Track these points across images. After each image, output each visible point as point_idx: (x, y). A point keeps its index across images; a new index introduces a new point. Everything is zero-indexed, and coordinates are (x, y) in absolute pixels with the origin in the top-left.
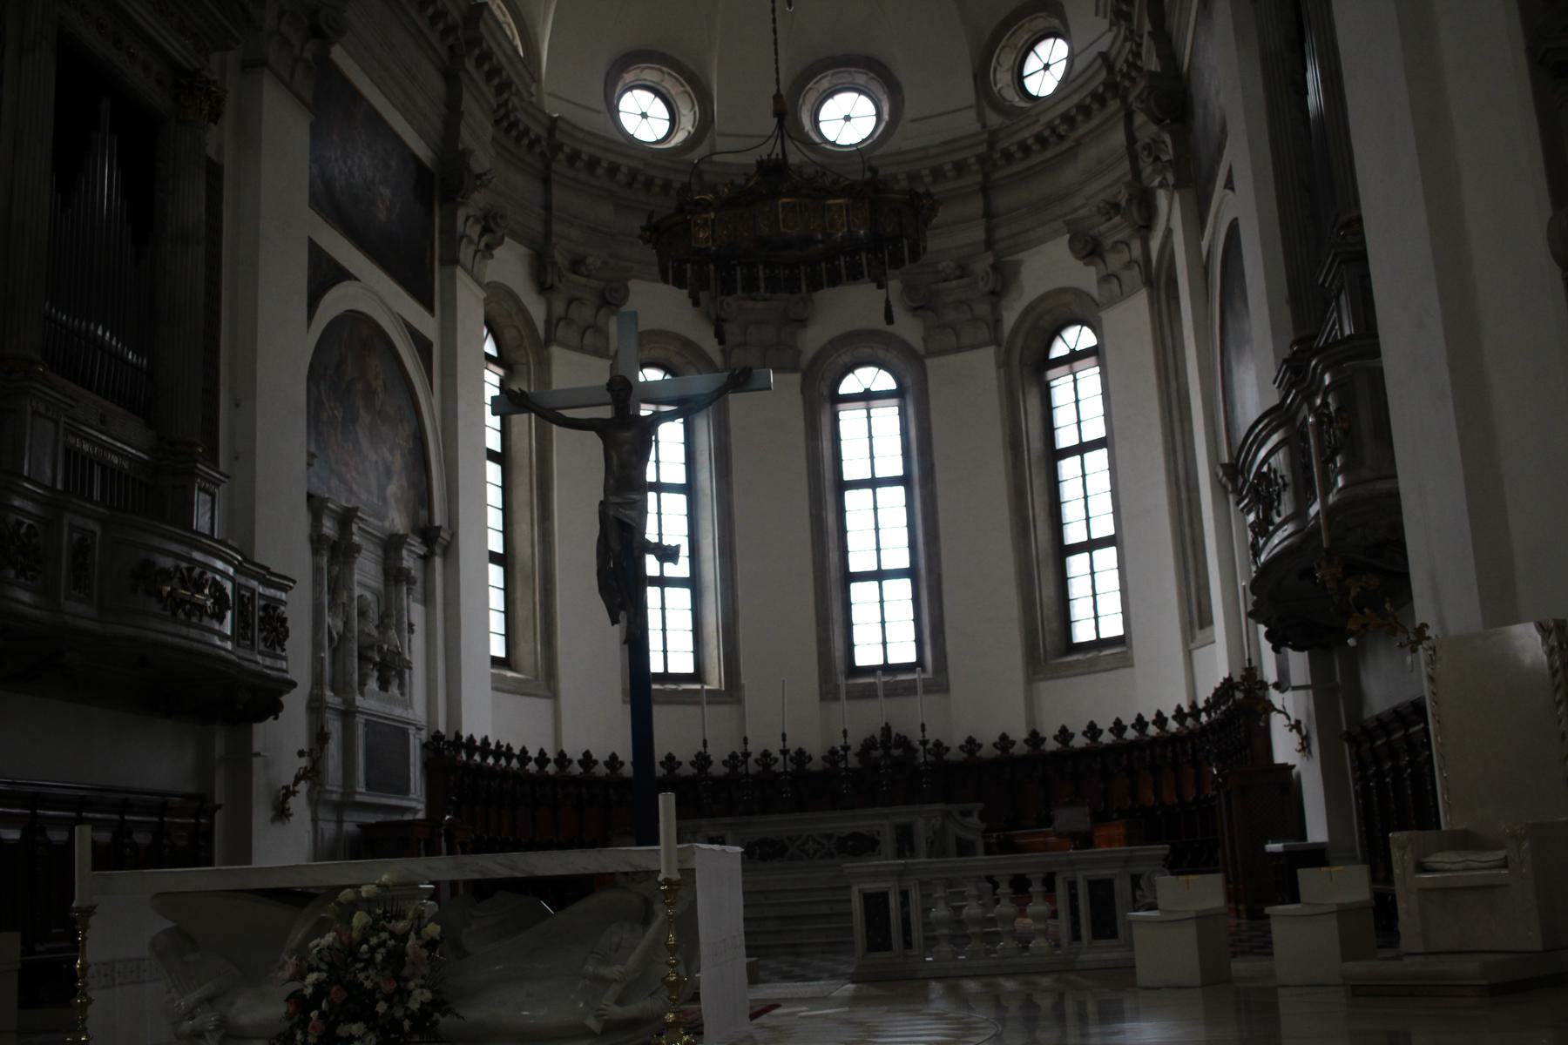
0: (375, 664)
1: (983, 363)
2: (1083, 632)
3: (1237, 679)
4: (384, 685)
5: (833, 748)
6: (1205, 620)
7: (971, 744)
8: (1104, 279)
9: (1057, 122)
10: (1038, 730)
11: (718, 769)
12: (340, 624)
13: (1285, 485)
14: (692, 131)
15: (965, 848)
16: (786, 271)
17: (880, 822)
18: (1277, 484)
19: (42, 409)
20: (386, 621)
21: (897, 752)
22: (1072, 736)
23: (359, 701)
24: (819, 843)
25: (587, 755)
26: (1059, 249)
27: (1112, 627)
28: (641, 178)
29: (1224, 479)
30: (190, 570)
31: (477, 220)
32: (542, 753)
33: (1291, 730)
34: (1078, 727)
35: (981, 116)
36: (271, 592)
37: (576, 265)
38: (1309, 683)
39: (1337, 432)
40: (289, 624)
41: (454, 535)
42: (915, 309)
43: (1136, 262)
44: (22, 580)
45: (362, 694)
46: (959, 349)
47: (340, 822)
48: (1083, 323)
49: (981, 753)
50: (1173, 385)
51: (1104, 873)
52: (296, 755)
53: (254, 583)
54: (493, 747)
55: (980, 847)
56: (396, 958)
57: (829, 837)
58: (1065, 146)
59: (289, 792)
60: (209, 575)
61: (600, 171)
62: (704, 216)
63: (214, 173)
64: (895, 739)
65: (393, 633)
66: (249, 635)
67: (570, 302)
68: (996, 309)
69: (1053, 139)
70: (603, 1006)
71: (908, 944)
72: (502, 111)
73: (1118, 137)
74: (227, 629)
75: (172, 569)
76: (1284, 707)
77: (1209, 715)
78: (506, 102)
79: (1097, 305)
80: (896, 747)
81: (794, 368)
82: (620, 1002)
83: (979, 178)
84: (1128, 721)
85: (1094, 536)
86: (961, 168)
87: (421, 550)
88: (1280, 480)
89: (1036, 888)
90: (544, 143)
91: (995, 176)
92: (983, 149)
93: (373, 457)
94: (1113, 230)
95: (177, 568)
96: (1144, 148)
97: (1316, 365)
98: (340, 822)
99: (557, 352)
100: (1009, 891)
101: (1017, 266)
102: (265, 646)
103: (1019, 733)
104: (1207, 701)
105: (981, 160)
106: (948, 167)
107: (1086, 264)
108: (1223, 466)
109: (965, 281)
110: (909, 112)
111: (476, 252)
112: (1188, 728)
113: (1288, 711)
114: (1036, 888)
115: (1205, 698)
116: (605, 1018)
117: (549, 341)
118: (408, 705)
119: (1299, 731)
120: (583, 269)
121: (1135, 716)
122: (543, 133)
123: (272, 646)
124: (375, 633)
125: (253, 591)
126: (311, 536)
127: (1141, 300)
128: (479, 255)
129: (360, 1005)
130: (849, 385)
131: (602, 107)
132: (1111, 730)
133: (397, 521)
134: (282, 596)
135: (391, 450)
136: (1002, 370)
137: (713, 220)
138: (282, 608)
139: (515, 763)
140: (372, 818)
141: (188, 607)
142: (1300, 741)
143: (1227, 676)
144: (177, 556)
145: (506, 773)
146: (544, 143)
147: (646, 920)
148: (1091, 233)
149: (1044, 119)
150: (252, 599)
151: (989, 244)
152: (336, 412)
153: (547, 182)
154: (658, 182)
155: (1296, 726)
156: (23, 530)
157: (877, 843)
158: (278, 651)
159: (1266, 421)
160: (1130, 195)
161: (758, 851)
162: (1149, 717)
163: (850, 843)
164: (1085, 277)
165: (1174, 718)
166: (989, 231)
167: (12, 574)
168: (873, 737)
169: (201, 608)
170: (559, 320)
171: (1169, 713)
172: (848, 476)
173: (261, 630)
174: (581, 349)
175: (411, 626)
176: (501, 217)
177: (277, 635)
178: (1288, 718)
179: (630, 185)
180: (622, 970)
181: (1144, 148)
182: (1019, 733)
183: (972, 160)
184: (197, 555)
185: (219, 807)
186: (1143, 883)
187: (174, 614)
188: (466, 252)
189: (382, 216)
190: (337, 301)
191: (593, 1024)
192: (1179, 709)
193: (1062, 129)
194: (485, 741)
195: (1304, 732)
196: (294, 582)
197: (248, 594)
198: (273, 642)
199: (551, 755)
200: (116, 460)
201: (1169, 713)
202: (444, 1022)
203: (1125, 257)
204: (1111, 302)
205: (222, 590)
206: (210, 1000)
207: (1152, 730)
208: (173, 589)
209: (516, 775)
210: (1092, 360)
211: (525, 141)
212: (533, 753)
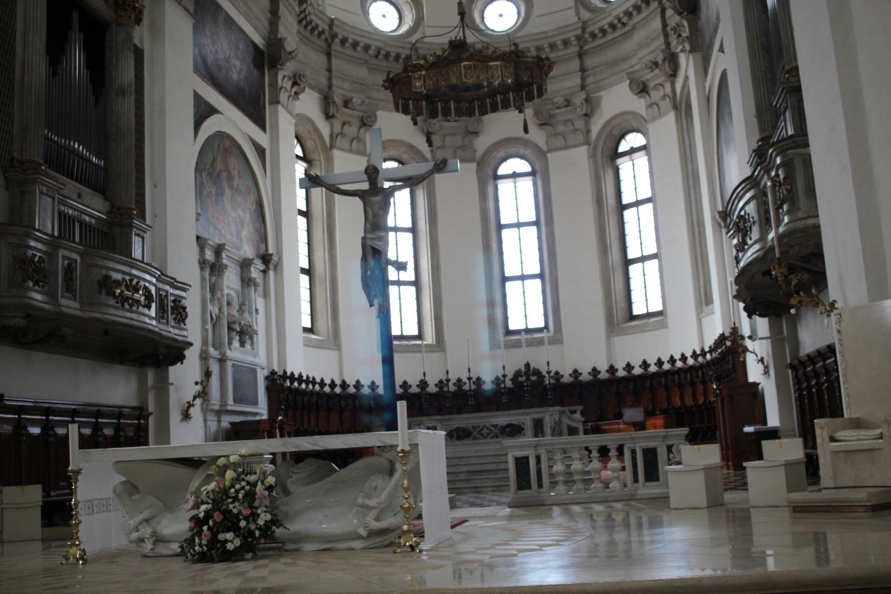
0: (237, 332)
1: (580, 155)
2: (638, 309)
3: (727, 334)
4: (242, 344)
5: (497, 376)
6: (709, 301)
8: (650, 106)
9: (622, 15)
10: (614, 365)
11: (432, 389)
12: (216, 310)
13: (754, 222)
14: (412, 24)
15: (572, 431)
16: (467, 104)
17: (525, 418)
18: (750, 222)
19: (45, 190)
20: (243, 307)
21: (533, 378)
22: (633, 368)
23: (229, 353)
24: (490, 430)
25: (358, 382)
26: (623, 88)
27: (656, 305)
28: (383, 53)
29: (719, 220)
30: (131, 280)
31: (290, 78)
32: (333, 381)
33: (758, 363)
34: (636, 363)
35: (578, 13)
36: (177, 292)
37: (347, 103)
38: (768, 335)
39: (784, 191)
40: (187, 310)
41: (280, 259)
42: (541, 125)
43: (668, 96)
44: (37, 287)
45: (230, 349)
46: (567, 147)
47: (219, 421)
48: (637, 131)
49: (581, 378)
50: (690, 166)
51: (651, 444)
52: (194, 385)
53: (167, 288)
54: (305, 378)
55: (581, 430)
56: (250, 496)
57: (496, 426)
58: (626, 29)
59: (190, 405)
60: (142, 283)
61: (359, 49)
62: (419, 73)
63: (139, 54)
64: (533, 371)
65: (246, 315)
66: (166, 317)
67: (344, 124)
68: (587, 123)
69: (619, 25)
70: (368, 522)
71: (540, 485)
72: (303, 15)
73: (657, 24)
74: (153, 312)
75: (121, 280)
76: (754, 350)
77: (711, 355)
78: (304, 10)
79: (646, 121)
80: (534, 374)
81: (472, 160)
82: (377, 519)
83: (577, 49)
84: (665, 359)
85: (645, 254)
86: (566, 43)
87: (262, 267)
88: (751, 220)
89: (613, 453)
90: (327, 33)
91: (586, 48)
92: (579, 32)
93: (233, 215)
94: (655, 78)
95: (124, 279)
96: (672, 30)
97: (772, 154)
98: (219, 421)
99: (336, 153)
100: (598, 455)
101: (599, 99)
102: (175, 323)
103: (603, 367)
104: (710, 347)
105: (578, 38)
106: (559, 43)
107: (639, 97)
108: (719, 212)
109: (569, 108)
110: (536, 11)
111: (289, 96)
112: (699, 362)
113: (756, 352)
114: (613, 453)
115: (709, 345)
116: (369, 528)
117: (332, 147)
118: (256, 355)
119: (763, 363)
120: (350, 105)
121: (669, 356)
122: (326, 28)
123: (179, 322)
124: (236, 314)
125: (167, 292)
126: (199, 260)
127: (671, 117)
128: (291, 98)
129: (231, 523)
130: (503, 169)
131: (359, 11)
132: (655, 364)
133: (248, 251)
134: (183, 294)
135: (243, 211)
136: (591, 160)
137: (424, 76)
138: (184, 301)
139: (317, 387)
140: (237, 419)
141: (130, 301)
142: (763, 369)
143: (721, 332)
144: (123, 273)
145: (312, 393)
146: (327, 33)
147: (391, 473)
148: (642, 79)
149: (614, 14)
150: (166, 296)
151: (583, 87)
152: (211, 189)
153: (329, 55)
154: (393, 55)
155: (762, 360)
156: (36, 259)
157: (523, 429)
158: (182, 325)
159: (743, 185)
160: (664, 57)
161: (455, 435)
162: (677, 356)
163: (507, 430)
164: (639, 105)
165: (692, 357)
166: (583, 79)
167: (31, 284)
168: (520, 369)
169: (138, 302)
170: (338, 135)
171: (688, 354)
172: (503, 222)
173: (172, 314)
174: (350, 151)
175: (257, 310)
176: (303, 76)
177: (181, 317)
178: (757, 356)
179: (376, 56)
180: (378, 501)
181: (672, 30)
182: (603, 367)
183: (573, 39)
184: (135, 272)
185: (151, 414)
186: (674, 450)
187: (123, 305)
188: (283, 97)
189: (235, 77)
190: (211, 126)
191: (363, 532)
192: (694, 352)
193: (625, 20)
194: (300, 375)
195: (766, 364)
196: (190, 286)
197: (164, 294)
198: (179, 321)
199: (338, 382)
200: (87, 219)
201: (688, 354)
202: (279, 532)
203: (661, 93)
204: (654, 119)
205: (149, 291)
206: (147, 520)
207: (679, 364)
208: (122, 292)
209: (318, 393)
210: (643, 153)
211: (316, 32)
212: (327, 381)
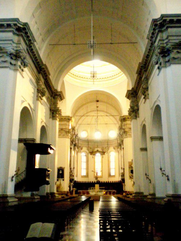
7: (104, 182)
11: (89, 182)
86: (106, 141)
94: (116, 148)
103: (107, 181)
151: (107, 146)
182: (107, 181)
